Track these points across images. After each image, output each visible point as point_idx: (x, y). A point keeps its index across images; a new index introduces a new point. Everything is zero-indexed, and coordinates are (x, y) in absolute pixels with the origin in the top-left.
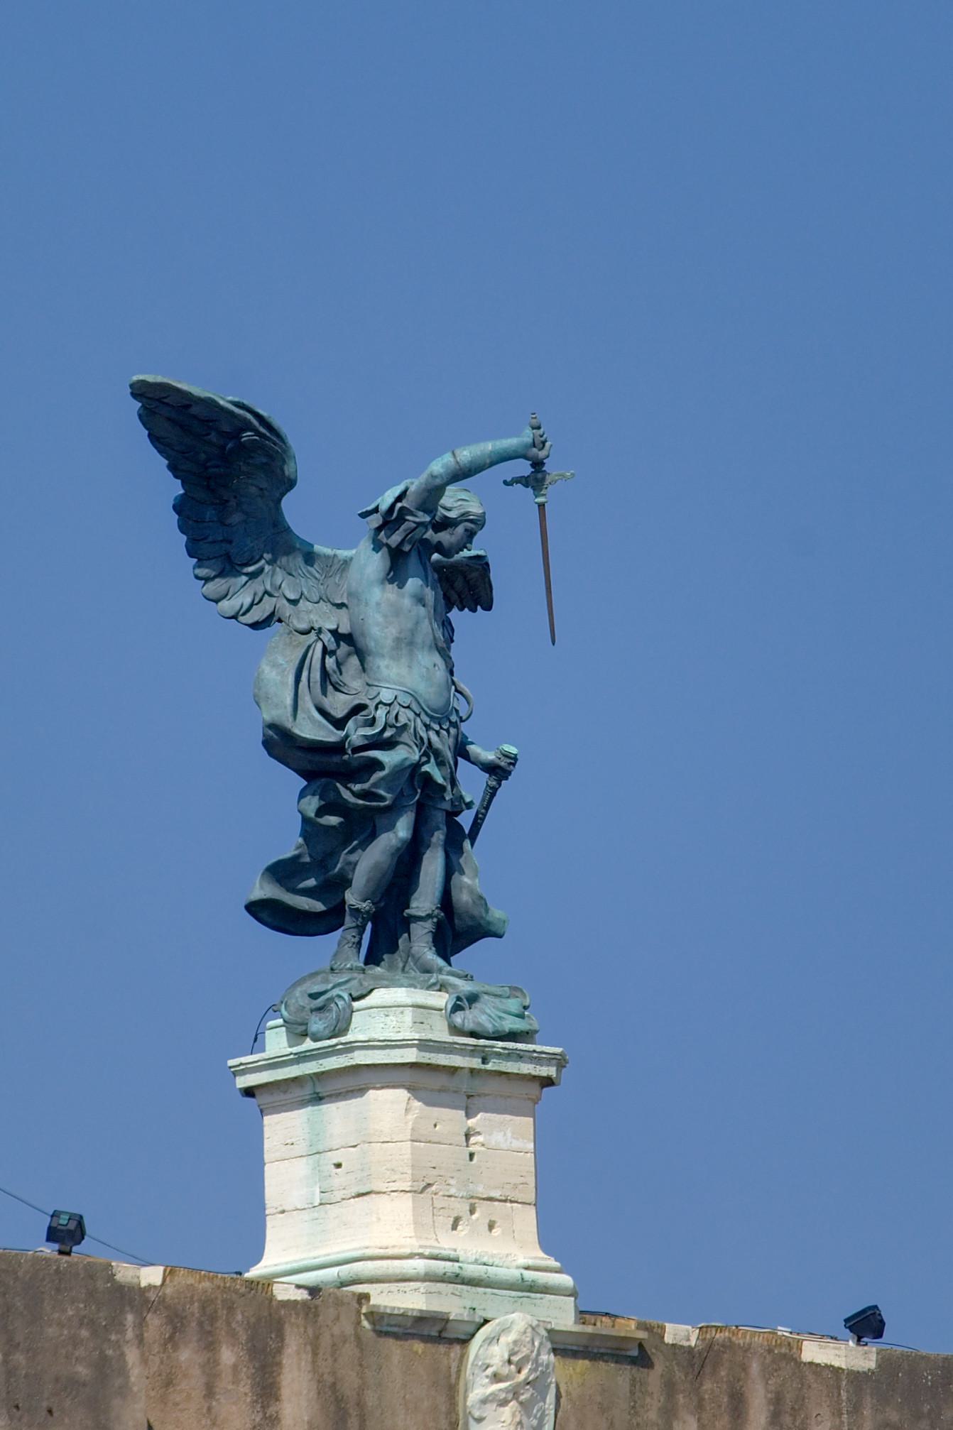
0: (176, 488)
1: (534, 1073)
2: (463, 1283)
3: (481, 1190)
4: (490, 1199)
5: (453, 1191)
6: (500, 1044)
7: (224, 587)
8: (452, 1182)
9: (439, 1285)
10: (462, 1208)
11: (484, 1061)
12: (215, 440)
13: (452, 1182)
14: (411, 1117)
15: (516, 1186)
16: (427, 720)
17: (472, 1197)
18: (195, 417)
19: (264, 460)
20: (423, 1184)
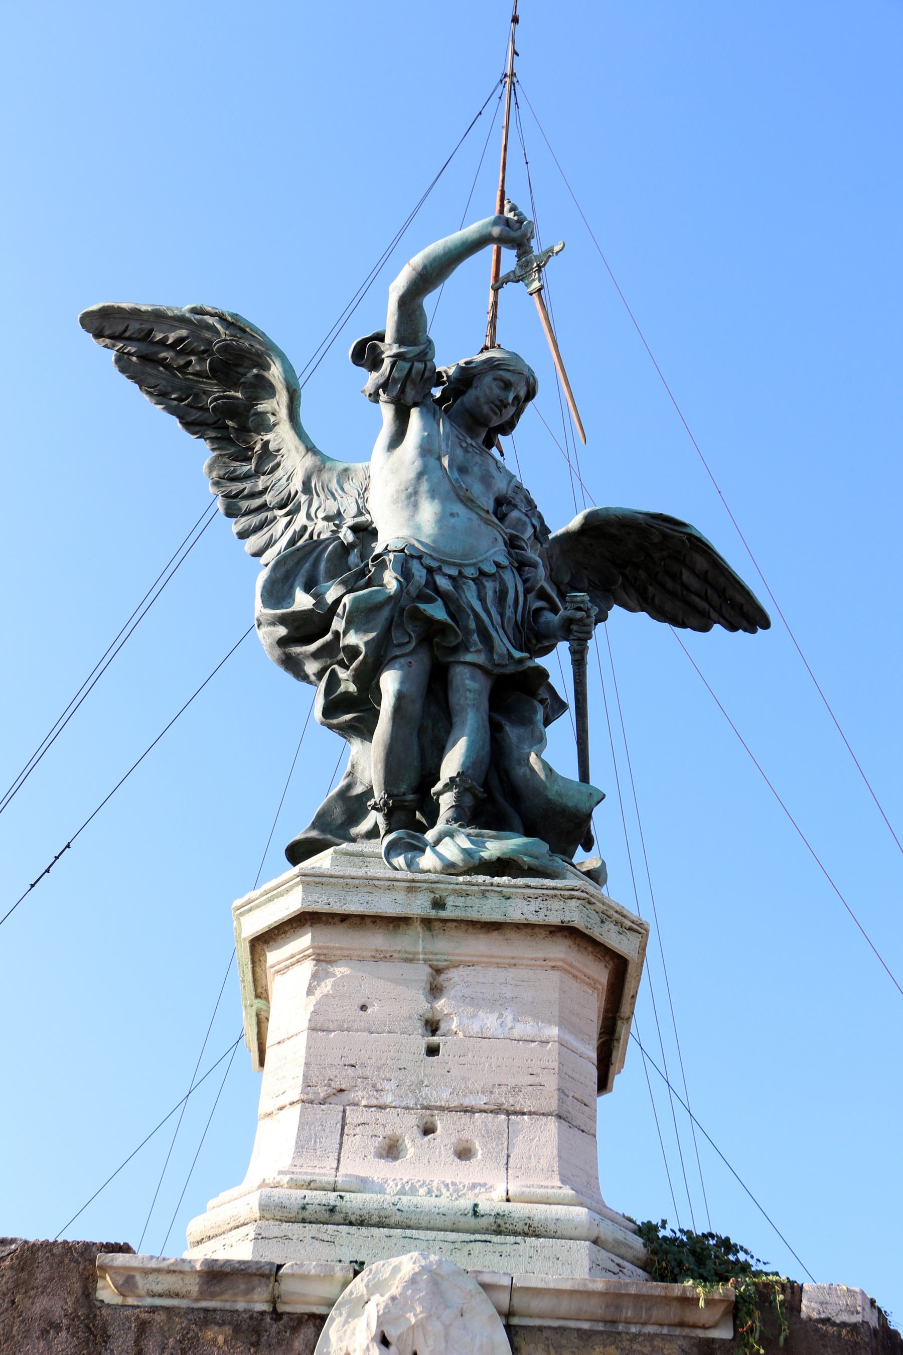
0: (200, 452)
1: (533, 919)
2: (351, 1224)
3: (443, 1096)
4: (468, 1110)
5: (388, 1099)
6: (461, 879)
8: (387, 1086)
10: (405, 1126)
11: (439, 904)
14: (318, 994)
15: (516, 1090)
16: (434, 564)
17: (427, 1108)
20: (322, 1092)
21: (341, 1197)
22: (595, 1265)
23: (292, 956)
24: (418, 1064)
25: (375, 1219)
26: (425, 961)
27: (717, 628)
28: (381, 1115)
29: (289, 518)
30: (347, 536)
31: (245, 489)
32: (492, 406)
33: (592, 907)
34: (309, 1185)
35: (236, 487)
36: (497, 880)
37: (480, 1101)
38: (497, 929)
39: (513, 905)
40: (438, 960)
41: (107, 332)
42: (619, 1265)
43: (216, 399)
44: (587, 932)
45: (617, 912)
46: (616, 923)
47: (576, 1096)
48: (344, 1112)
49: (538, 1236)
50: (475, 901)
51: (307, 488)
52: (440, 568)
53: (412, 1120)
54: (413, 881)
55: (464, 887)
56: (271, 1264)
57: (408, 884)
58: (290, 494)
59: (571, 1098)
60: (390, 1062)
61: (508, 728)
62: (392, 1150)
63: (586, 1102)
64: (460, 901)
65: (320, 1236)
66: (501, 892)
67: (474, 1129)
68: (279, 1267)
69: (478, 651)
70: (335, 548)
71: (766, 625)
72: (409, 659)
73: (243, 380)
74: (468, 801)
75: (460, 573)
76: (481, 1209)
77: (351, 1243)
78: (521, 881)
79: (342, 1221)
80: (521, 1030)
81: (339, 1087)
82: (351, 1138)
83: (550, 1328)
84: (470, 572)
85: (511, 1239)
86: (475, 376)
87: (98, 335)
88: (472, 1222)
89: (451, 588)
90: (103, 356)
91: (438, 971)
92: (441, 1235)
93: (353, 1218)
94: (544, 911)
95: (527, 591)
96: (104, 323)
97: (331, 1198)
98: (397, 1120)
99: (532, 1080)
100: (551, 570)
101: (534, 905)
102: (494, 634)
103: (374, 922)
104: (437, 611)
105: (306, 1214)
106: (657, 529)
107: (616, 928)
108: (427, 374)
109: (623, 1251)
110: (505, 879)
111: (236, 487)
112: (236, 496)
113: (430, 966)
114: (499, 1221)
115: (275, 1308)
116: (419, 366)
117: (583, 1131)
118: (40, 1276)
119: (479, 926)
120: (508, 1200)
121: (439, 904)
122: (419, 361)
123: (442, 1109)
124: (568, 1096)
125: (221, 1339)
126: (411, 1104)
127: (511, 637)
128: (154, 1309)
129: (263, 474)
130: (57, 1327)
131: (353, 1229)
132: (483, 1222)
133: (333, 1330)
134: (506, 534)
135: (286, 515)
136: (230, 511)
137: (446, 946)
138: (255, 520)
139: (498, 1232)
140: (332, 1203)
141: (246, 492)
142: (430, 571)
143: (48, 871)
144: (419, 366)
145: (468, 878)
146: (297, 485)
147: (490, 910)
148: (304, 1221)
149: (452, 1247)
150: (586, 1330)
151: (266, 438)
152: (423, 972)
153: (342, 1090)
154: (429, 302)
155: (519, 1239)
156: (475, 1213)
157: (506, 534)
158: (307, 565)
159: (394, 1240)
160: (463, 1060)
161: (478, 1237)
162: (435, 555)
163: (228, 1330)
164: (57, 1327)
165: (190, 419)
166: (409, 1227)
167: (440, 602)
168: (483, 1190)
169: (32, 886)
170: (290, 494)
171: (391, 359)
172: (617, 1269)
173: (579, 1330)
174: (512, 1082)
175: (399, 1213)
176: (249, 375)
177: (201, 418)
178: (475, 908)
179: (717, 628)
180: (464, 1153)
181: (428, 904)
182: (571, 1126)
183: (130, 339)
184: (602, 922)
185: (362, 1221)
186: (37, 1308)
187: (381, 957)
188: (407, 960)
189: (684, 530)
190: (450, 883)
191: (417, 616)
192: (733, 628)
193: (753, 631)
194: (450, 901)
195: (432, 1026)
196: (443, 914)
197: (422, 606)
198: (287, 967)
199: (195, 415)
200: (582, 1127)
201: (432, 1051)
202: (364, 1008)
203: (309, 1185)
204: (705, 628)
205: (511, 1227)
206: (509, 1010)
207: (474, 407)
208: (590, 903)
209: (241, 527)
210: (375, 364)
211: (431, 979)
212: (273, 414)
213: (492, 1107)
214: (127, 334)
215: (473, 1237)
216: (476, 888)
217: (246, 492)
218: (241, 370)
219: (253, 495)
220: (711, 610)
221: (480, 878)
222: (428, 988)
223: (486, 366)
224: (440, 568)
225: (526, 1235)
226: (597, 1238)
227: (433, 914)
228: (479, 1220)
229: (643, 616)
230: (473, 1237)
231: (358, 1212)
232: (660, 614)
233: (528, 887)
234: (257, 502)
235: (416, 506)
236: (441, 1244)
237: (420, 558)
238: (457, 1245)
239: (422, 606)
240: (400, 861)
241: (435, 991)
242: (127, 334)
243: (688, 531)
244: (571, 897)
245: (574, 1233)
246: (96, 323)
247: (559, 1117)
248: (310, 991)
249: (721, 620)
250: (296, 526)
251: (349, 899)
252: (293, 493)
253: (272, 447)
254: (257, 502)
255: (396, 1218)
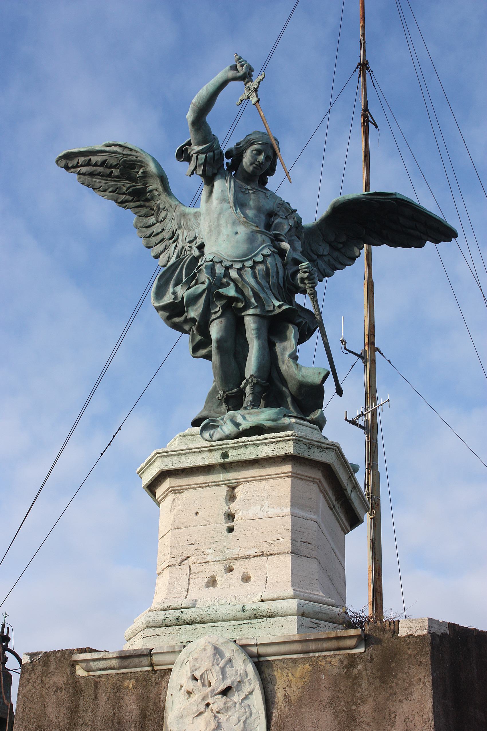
0: (130, 216)
1: (271, 454)
2: (188, 624)
3: (236, 552)
4: (248, 557)
5: (209, 558)
6: (233, 441)
7: (167, 256)
8: (209, 551)
9: (157, 629)
10: (218, 570)
11: (225, 455)
12: (116, 174)
13: (209, 551)
14: (175, 511)
15: (271, 543)
17: (229, 559)
18: (96, 165)
19: (141, 171)
20: (179, 560)
21: (182, 612)
22: (300, 627)
23: (164, 493)
24: (223, 538)
25: (198, 620)
26: (225, 484)
27: (429, 244)
28: (205, 566)
29: (175, 244)
30: (196, 252)
31: (153, 232)
32: (254, 165)
33: (302, 442)
34: (169, 609)
35: (149, 232)
36: (252, 438)
37: (252, 552)
38: (257, 462)
39: (261, 449)
40: (231, 483)
41: (70, 165)
42: (316, 623)
43: (129, 188)
44: (300, 455)
45: (317, 442)
46: (318, 447)
47: (303, 540)
48: (190, 567)
49: (274, 616)
50: (242, 451)
51: (180, 227)
52: (232, 265)
53: (222, 567)
54: (211, 446)
55: (236, 445)
56: (147, 649)
57: (208, 449)
58: (173, 231)
59: (299, 542)
60: (210, 539)
61: (277, 344)
62: (212, 582)
63: (309, 542)
64: (235, 452)
65: (173, 632)
66: (254, 444)
67: (252, 567)
68: (151, 650)
69: (255, 307)
70: (190, 260)
71: (455, 235)
72: (220, 319)
73: (138, 176)
74: (258, 389)
75: (243, 265)
76: (246, 608)
77: (186, 633)
78: (262, 437)
79: (183, 623)
80: (273, 512)
81: (187, 556)
82: (194, 580)
83: (278, 660)
84: (249, 263)
85: (260, 620)
86: (243, 151)
87: (67, 168)
88: (242, 614)
89: (237, 276)
90: (72, 179)
91: (234, 488)
92: (228, 623)
93: (188, 621)
94: (276, 449)
95: (284, 265)
96: (69, 161)
97: (177, 613)
98: (214, 567)
99: (279, 537)
100: (323, 236)
101: (271, 447)
102: (262, 295)
103: (198, 470)
104: (231, 291)
105: (166, 622)
106: (376, 201)
107: (319, 450)
108: (216, 158)
109: (320, 616)
110: (256, 437)
111: (149, 232)
112: (150, 236)
113: (228, 486)
114: (255, 612)
115: (153, 669)
116: (211, 154)
117: (308, 557)
118: (52, 667)
119: (248, 462)
120: (262, 601)
121: (225, 455)
122: (210, 152)
123: (236, 559)
124: (297, 542)
125: (131, 686)
126: (221, 558)
127: (277, 293)
128: (100, 676)
129: (160, 222)
130: (61, 689)
131: (187, 627)
132: (248, 614)
133: (173, 676)
134: (271, 235)
135: (174, 242)
136: (148, 245)
137: (232, 476)
138: (160, 247)
139: (256, 618)
140: (178, 615)
141: (154, 234)
142: (227, 268)
143: (110, 444)
144: (211, 154)
145: (236, 440)
146: (175, 227)
147: (250, 453)
148: (166, 626)
149: (233, 628)
150: (295, 659)
151: (158, 202)
152: (224, 489)
153: (189, 557)
154: (210, 118)
155: (264, 620)
156: (243, 610)
157: (271, 235)
158: (177, 273)
159: (206, 629)
160: (244, 532)
161: (245, 621)
162: (229, 259)
163: (133, 681)
164: (61, 689)
165: (120, 200)
166: (214, 622)
167: (232, 284)
168: (252, 597)
169: (102, 454)
170: (173, 231)
171: (196, 155)
172: (315, 626)
173: (291, 659)
174: (268, 540)
175: (208, 616)
176: (140, 172)
177: (126, 199)
178: (243, 455)
179: (428, 243)
180: (246, 579)
181: (219, 456)
182: (300, 556)
183: (82, 166)
184: (309, 448)
185: (192, 622)
186: (51, 682)
187: (204, 486)
188: (217, 485)
189: (392, 197)
190: (228, 444)
191: (220, 297)
192: (436, 241)
193: (450, 241)
194: (230, 453)
195: (231, 517)
196: (227, 460)
197: (221, 291)
198: (163, 498)
199: (122, 198)
200: (307, 555)
201: (231, 530)
202: (197, 514)
203: (169, 609)
204: (421, 245)
205: (261, 614)
206: (266, 503)
207: (246, 169)
208: (299, 441)
209: (154, 253)
210: (188, 159)
211: (230, 493)
212: (156, 190)
213: (259, 554)
214: (80, 164)
215: (242, 622)
216: (241, 444)
217: (154, 234)
218: (135, 170)
219: (158, 234)
220: (422, 235)
221: (242, 439)
222: (229, 498)
223: (247, 144)
224: (232, 265)
225: (268, 617)
226: (303, 613)
227: (222, 460)
228: (245, 613)
229: (385, 246)
230: (242, 622)
231: (190, 618)
232: (394, 244)
233: (266, 439)
234: (160, 237)
235: (219, 233)
236: (228, 628)
237: (221, 262)
238: (235, 627)
239: (221, 291)
240: (206, 435)
241: (232, 497)
242: (80, 164)
243: (394, 197)
244: (289, 440)
245: (290, 613)
246: (63, 162)
247: (292, 553)
248: (172, 510)
249: (429, 239)
250: (179, 248)
251: (182, 461)
252: (175, 230)
253: (161, 206)
254: (160, 237)
255: (207, 618)
